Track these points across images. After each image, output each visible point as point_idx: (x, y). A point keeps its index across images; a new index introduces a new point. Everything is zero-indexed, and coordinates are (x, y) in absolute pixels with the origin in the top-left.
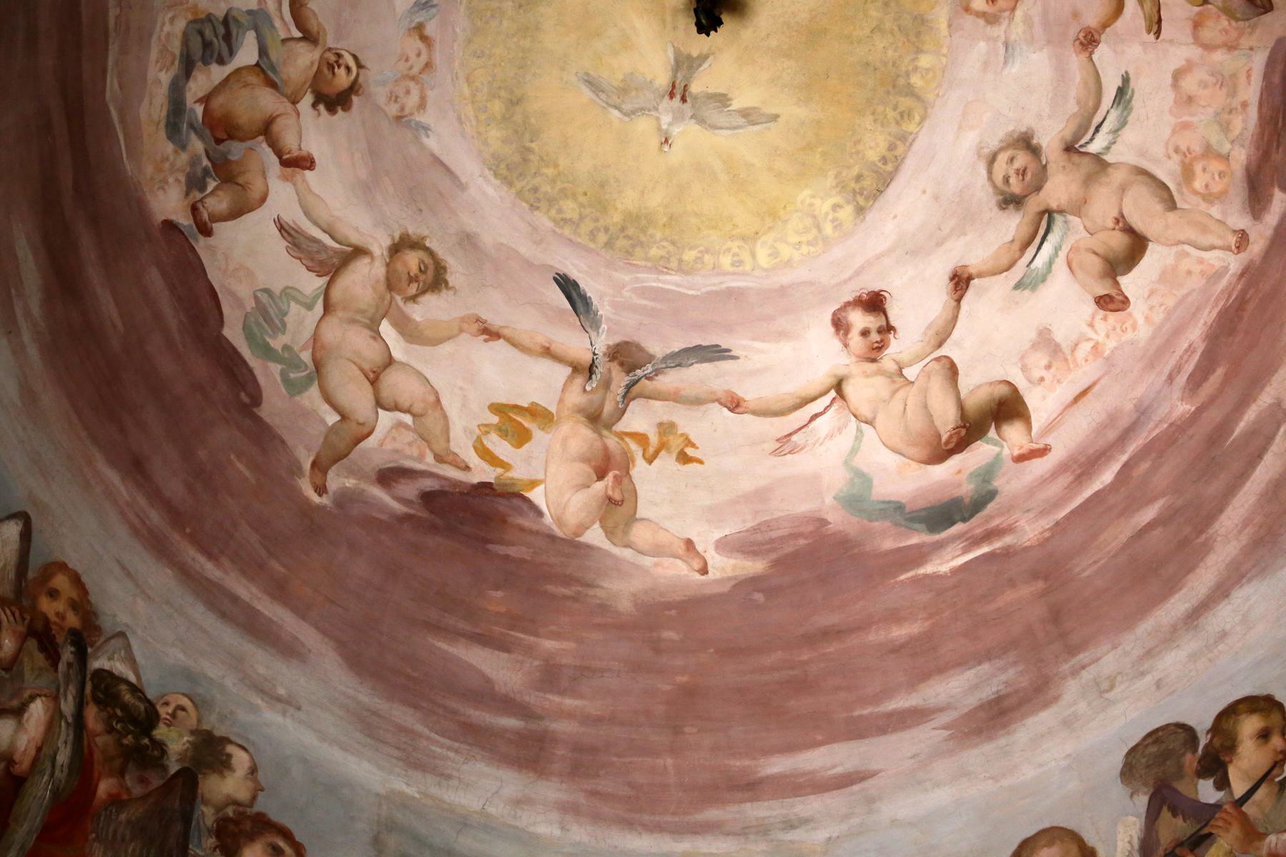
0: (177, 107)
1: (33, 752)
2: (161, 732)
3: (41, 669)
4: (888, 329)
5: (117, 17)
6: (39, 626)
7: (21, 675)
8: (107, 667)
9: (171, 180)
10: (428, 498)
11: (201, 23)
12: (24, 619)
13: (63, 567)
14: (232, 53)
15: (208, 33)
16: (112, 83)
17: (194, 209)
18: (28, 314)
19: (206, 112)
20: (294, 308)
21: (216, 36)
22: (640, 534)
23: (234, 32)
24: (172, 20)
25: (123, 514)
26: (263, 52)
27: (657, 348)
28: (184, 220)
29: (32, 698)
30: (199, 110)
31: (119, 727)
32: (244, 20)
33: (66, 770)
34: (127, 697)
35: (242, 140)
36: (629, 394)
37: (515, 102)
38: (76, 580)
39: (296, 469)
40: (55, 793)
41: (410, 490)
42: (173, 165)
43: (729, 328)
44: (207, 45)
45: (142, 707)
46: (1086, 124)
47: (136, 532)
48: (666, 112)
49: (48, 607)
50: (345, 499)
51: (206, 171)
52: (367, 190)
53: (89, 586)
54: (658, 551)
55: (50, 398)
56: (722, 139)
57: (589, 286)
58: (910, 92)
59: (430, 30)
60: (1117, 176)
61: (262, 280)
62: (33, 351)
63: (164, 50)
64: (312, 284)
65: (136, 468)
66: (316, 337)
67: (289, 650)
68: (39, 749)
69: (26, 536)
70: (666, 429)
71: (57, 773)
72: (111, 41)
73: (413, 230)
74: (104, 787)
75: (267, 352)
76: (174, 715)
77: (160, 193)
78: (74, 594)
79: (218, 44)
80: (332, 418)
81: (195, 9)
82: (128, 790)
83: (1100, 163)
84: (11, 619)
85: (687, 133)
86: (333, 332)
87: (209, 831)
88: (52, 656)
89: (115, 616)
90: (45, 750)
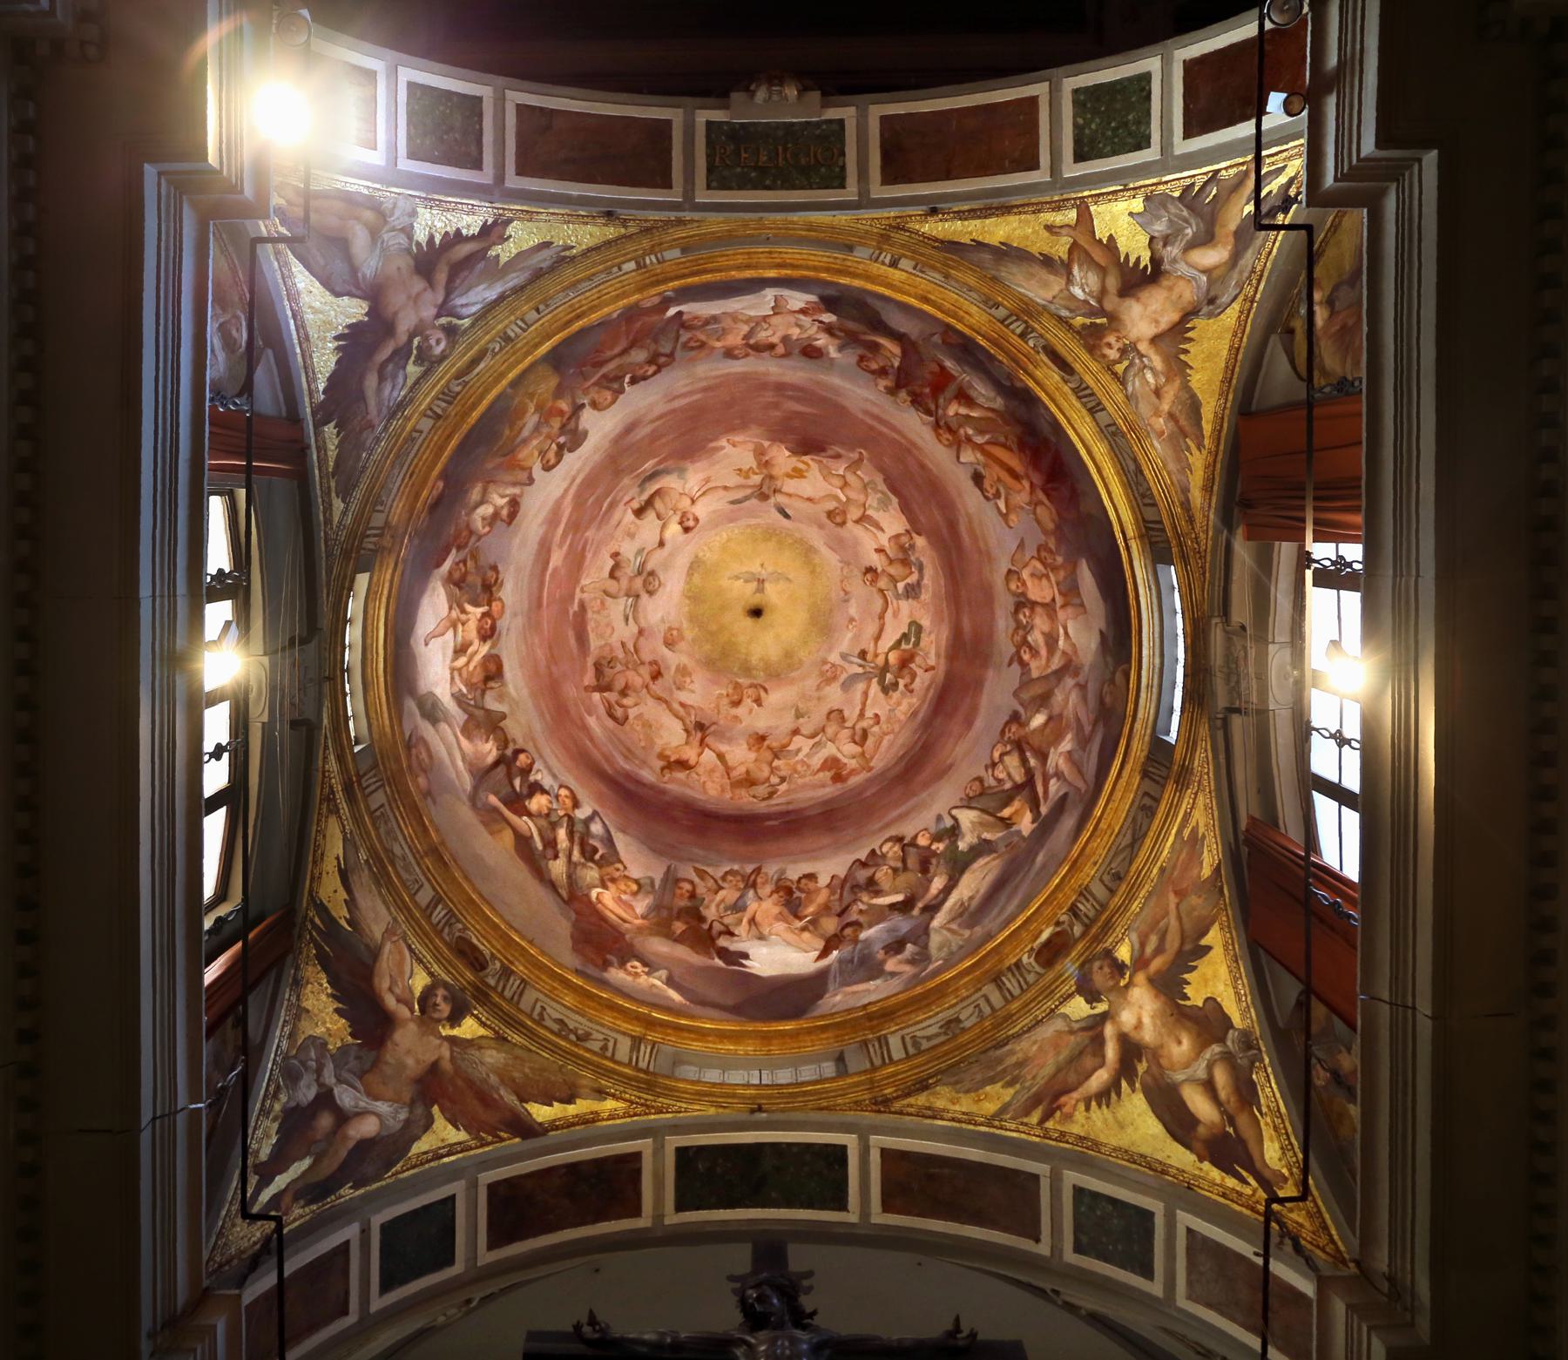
0: (921, 569)
4: (681, 523)
10: (823, 450)
16: (942, 582)
20: (875, 505)
22: (751, 446)
26: (896, 587)
27: (754, 501)
28: (914, 535)
36: (761, 486)
37: (813, 572)
39: (870, 460)
41: (830, 452)
43: (732, 511)
46: (635, 606)
48: (764, 574)
50: (852, 449)
52: (856, 543)
54: (745, 442)
56: (745, 569)
57: (780, 517)
58: (689, 598)
59: (842, 593)
60: (622, 593)
61: (887, 515)
62: (959, 506)
64: (870, 512)
65: (923, 466)
66: (867, 496)
67: (866, 412)
69: (958, 458)
70: (747, 477)
73: (839, 529)
74: (927, 390)
75: (882, 493)
80: (859, 473)
83: (628, 595)
85: (755, 568)
86: (862, 498)
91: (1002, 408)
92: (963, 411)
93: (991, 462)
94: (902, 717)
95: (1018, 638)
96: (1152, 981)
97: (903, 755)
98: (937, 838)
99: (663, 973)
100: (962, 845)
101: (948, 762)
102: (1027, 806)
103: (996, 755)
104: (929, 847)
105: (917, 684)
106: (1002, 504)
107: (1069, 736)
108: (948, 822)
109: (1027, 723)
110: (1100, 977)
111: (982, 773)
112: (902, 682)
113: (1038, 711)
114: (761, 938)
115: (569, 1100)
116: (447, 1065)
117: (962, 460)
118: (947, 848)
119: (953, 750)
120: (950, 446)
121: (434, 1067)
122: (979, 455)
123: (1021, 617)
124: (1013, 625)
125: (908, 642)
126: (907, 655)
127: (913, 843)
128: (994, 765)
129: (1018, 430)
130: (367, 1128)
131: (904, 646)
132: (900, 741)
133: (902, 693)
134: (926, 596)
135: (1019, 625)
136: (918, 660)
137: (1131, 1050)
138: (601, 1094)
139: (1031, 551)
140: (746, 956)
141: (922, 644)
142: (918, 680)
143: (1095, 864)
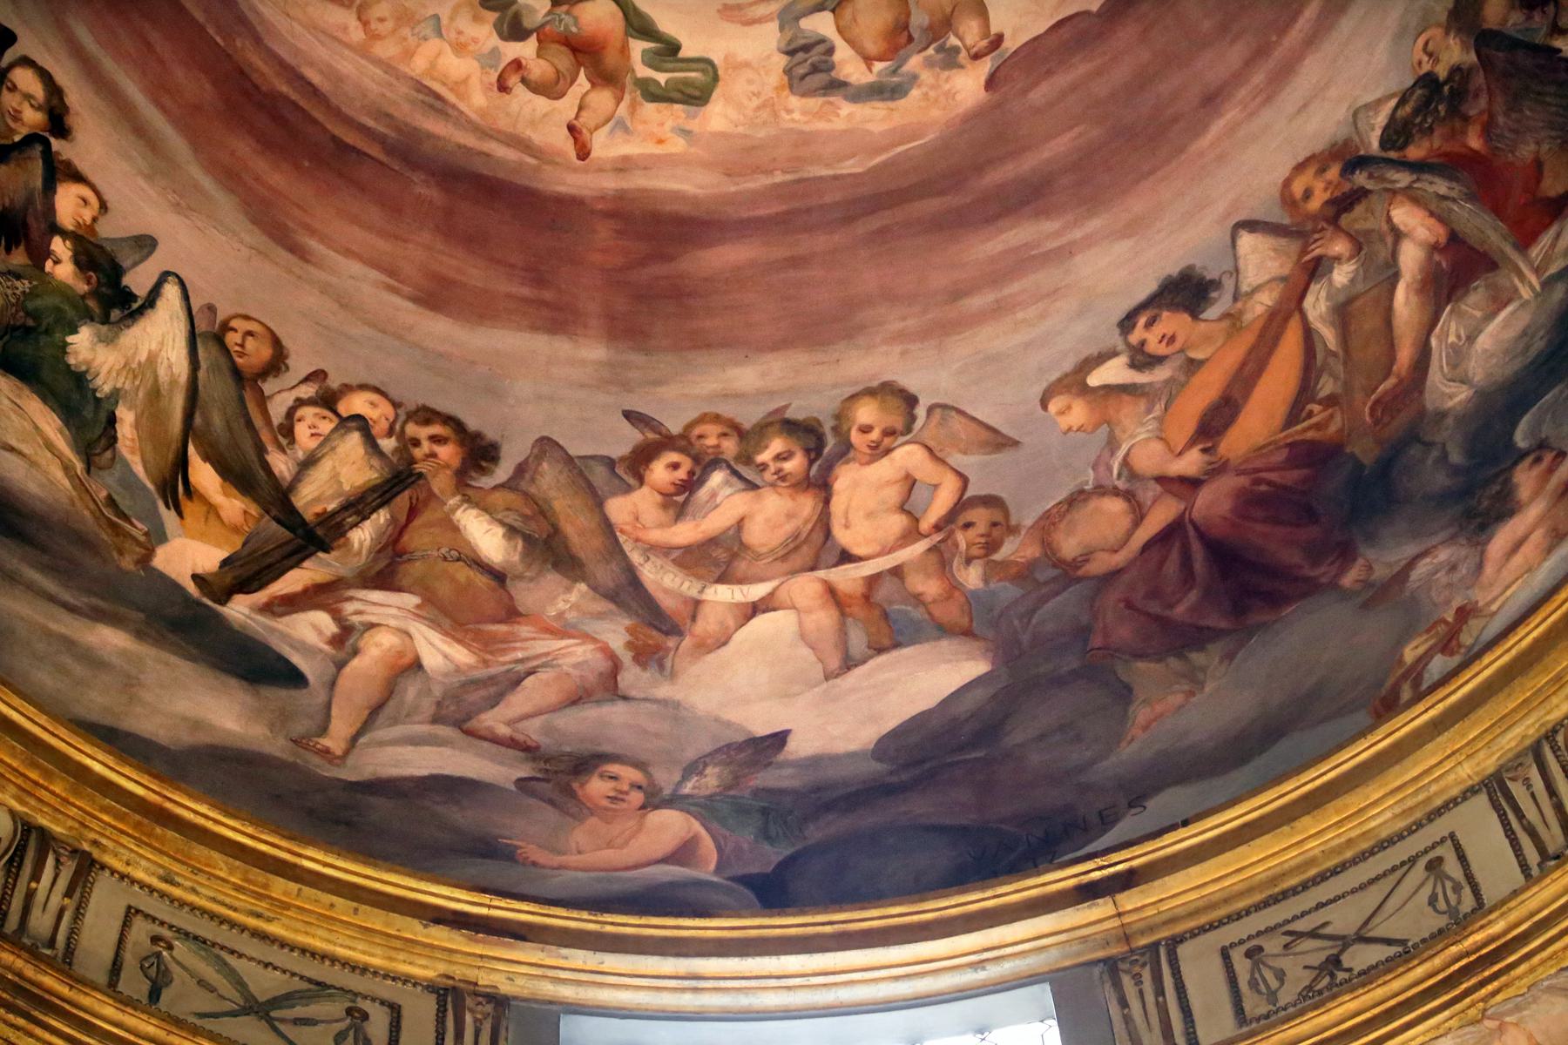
1: (1432, 221)
2: (1442, 72)
3: (1367, 210)
5: (784, 172)
6: (1331, 211)
7: (1368, 233)
8: (1378, 132)
9: (947, 87)
11: (795, 81)
12: (1323, 229)
13: (1287, 183)
14: (822, 41)
15: (801, 70)
16: (850, 167)
17: (976, 57)
18: (1057, 234)
19: (880, 59)
21: (806, 61)
23: (802, 42)
24: (789, 111)
25: (1252, 114)
28: (986, 66)
29: (1389, 219)
30: (879, 66)
31: (1429, 120)
32: (789, 34)
33: (1454, 185)
34: (1408, 109)
35: (908, 14)
38: (1300, 168)
40: (1471, 198)
42: (933, 87)
44: (815, 69)
45: (1419, 92)
47: (1269, 99)
49: (1315, 204)
51: (938, 51)
53: (1307, 153)
55: (1136, 204)
62: (1094, 224)
63: (818, 115)
65: (1212, 100)
68: (1432, 214)
69: (1251, 225)
71: (1454, 194)
72: (806, 175)
74: (1475, 142)
76: (1430, 55)
77: (958, 97)
78: (1311, 171)
79: (815, 56)
81: (778, 89)
82: (1482, 113)
84: (1318, 243)
87: (1529, 18)
88: (1360, 194)
89: (1339, 122)
90: (1433, 207)
91: (1431, 401)
92: (1411, 258)
93: (1248, 339)
94: (418, 66)
95: (711, 436)
97: (313, 91)
98: (92, 255)
100: (83, 344)
101: (313, 244)
102: (238, 542)
103: (357, 404)
104: (55, 229)
105: (524, 102)
106: (1113, 372)
107: (462, 655)
108: (138, 280)
109: (467, 500)
111: (300, 365)
112: (526, 50)
113: (512, 531)
117: (1246, 241)
118: (63, 291)
119: (348, 253)
120: (1287, 199)
122: (1265, 301)
123: (777, 445)
124: (749, 416)
125: (653, 61)
126: (611, 59)
127: (58, 172)
128: (328, 400)
129: (1365, 450)
131: (638, 47)
132: (347, 65)
133: (495, 52)
134: (799, 111)
135: (750, 438)
136: (603, 99)
139: (985, 473)
141: (650, 109)
142: (541, 103)
143: (168, 880)
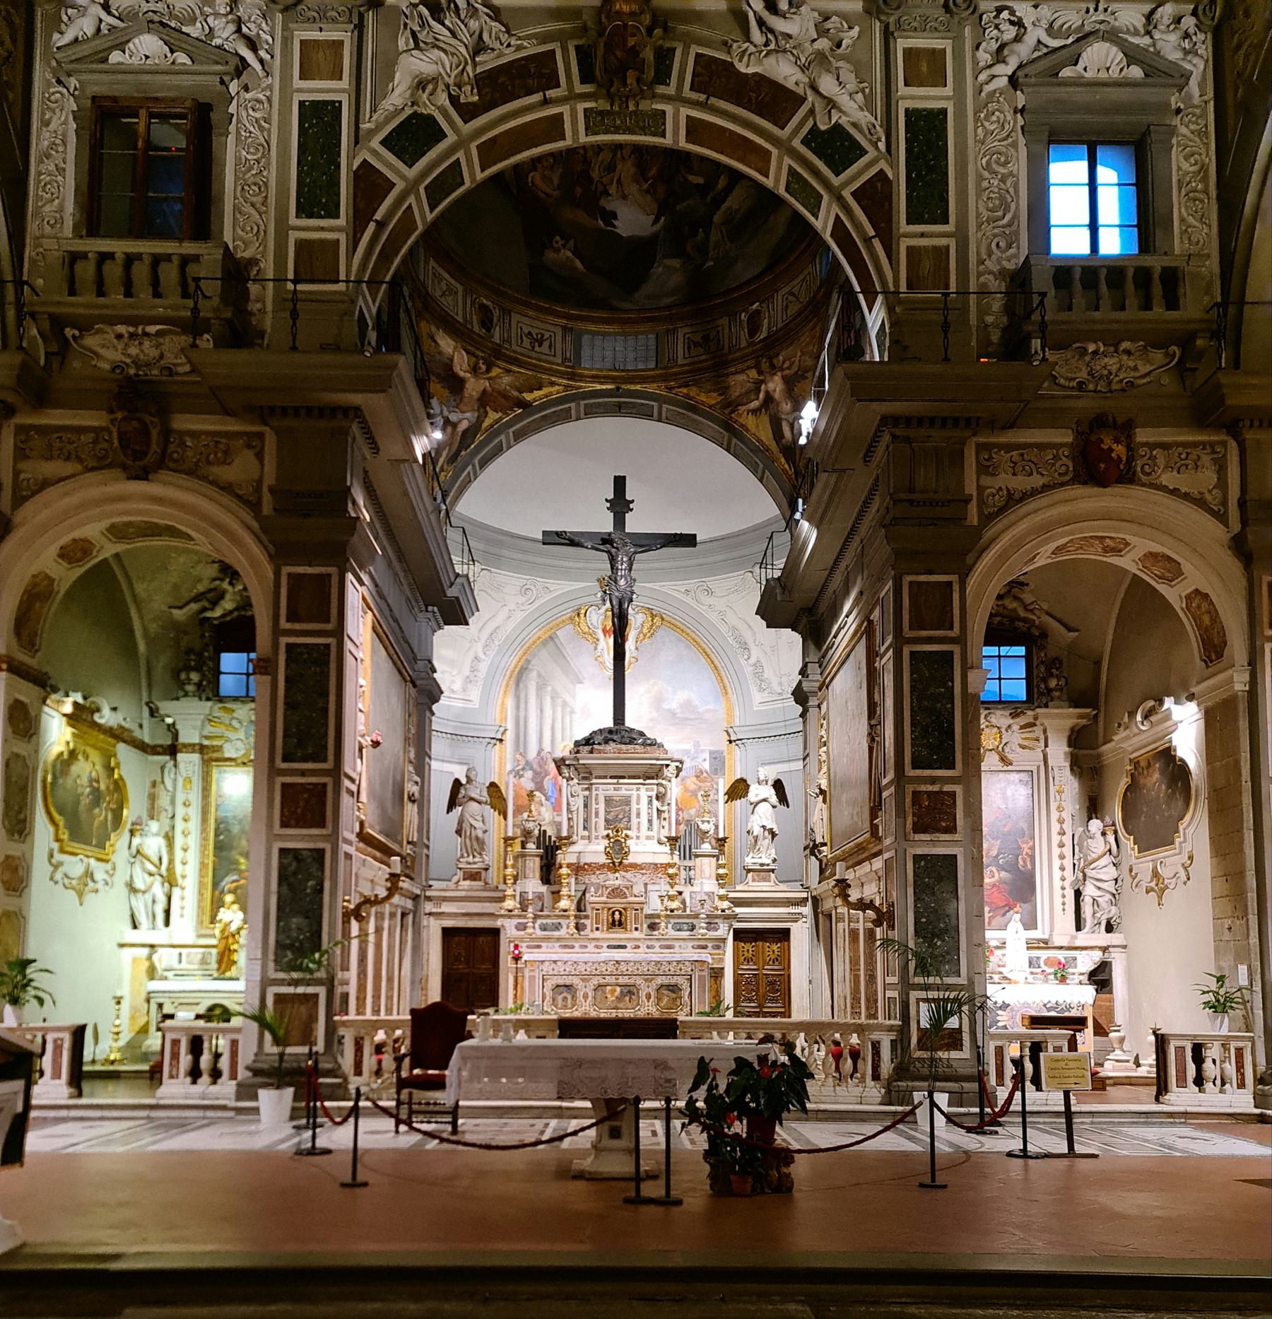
96: (783, 377)
99: (571, 243)
110: (765, 365)
114: (624, 197)
115: (540, 389)
116: (489, 389)
121: (484, 391)
130: (464, 425)
137: (769, 399)
138: (553, 384)
140: (614, 215)
